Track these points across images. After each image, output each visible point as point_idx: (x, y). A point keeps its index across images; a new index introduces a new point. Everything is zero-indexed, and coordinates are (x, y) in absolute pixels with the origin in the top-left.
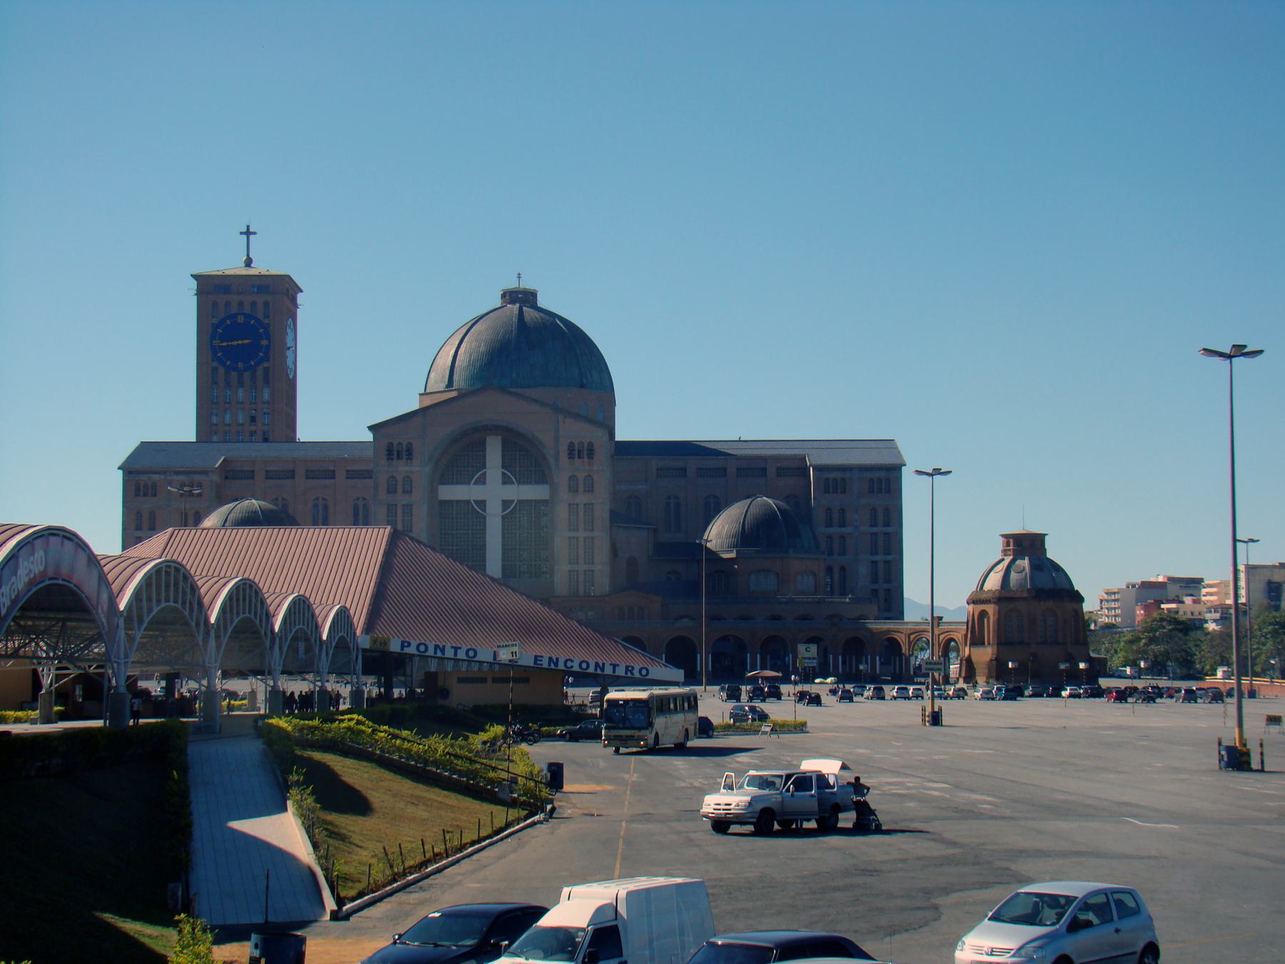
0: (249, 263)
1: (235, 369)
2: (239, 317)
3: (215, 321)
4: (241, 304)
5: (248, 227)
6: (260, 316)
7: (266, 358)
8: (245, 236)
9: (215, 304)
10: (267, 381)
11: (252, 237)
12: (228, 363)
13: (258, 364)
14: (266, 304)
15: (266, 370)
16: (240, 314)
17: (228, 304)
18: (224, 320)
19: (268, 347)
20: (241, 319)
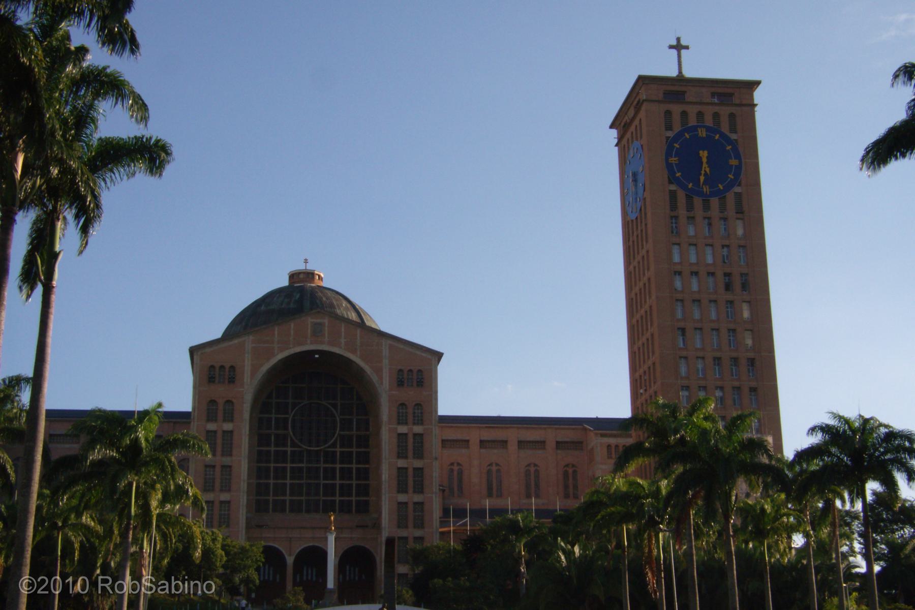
1: (700, 194)
2: (700, 130)
4: (700, 115)
7: (736, 182)
8: (674, 52)
9: (668, 113)
10: (740, 211)
11: (683, 52)
12: (690, 186)
14: (732, 116)
15: (738, 196)
16: (700, 127)
17: (684, 114)
18: (679, 135)
19: (739, 168)
20: (702, 133)
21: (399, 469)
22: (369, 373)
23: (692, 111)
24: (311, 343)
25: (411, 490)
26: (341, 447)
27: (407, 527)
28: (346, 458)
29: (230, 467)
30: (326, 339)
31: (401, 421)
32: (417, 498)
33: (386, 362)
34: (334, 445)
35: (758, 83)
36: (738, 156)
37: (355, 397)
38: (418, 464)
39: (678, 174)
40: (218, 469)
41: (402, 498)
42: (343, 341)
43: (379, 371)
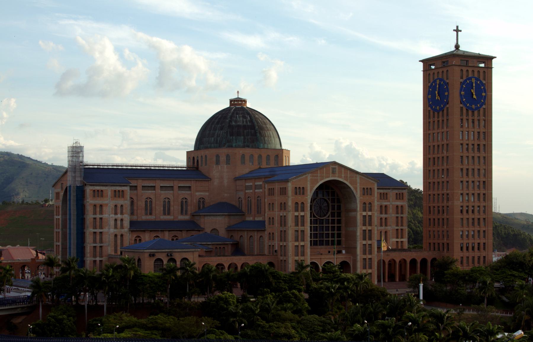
0: (457, 47)
3: (462, 80)
4: (473, 71)
5: (457, 27)
6: (481, 78)
7: (484, 103)
8: (455, 32)
9: (462, 70)
11: (459, 33)
13: (481, 106)
16: (473, 77)
17: (467, 71)
19: (485, 97)
21: (363, 230)
22: (353, 190)
23: (470, 70)
24: (332, 177)
25: (367, 239)
26: (331, 217)
27: (366, 254)
28: (333, 222)
29: (304, 231)
30: (337, 175)
31: (365, 210)
32: (369, 242)
33: (358, 185)
34: (329, 217)
35: (495, 57)
36: (485, 92)
37: (336, 195)
38: (370, 228)
39: (464, 100)
40: (300, 232)
41: (364, 242)
42: (343, 175)
43: (356, 189)
